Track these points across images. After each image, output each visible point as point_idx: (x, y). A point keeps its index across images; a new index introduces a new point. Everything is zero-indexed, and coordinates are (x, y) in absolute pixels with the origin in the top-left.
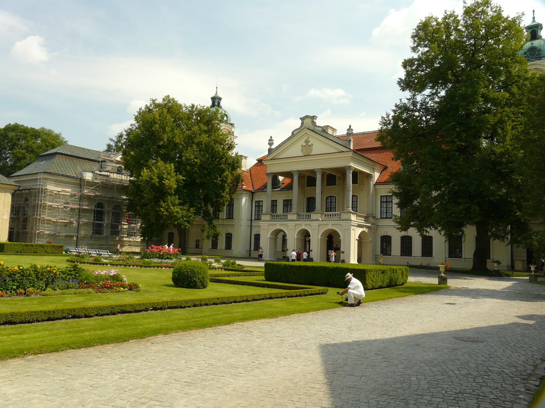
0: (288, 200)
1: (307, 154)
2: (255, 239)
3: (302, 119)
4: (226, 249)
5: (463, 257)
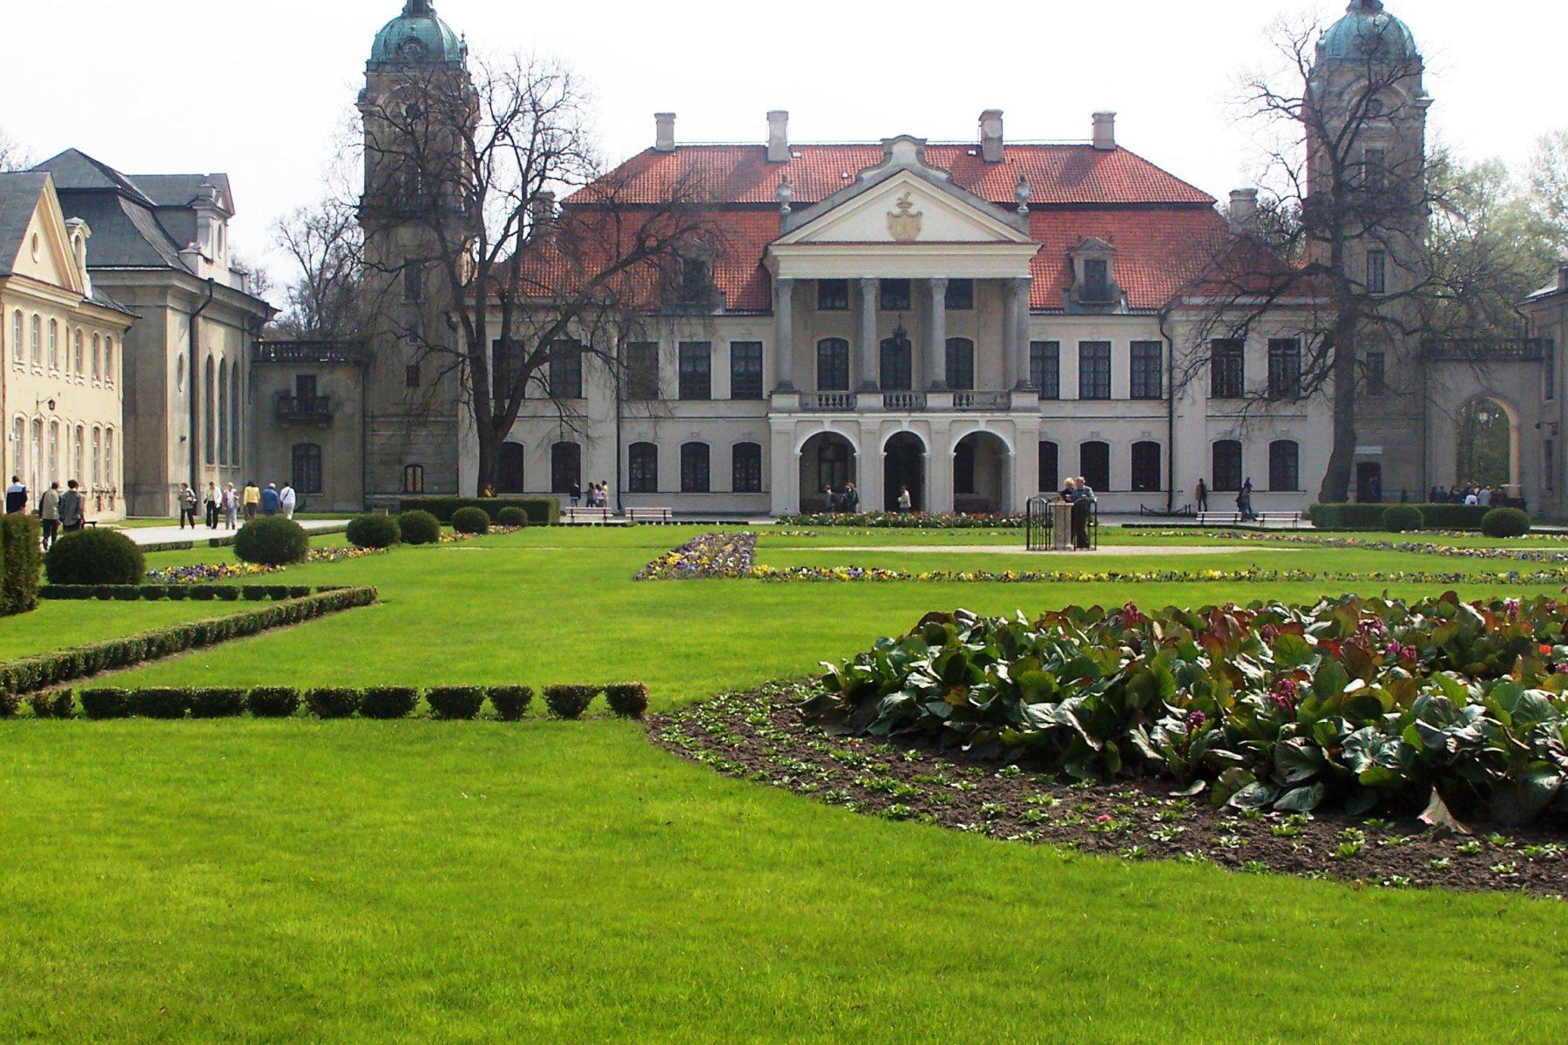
1: (902, 238)
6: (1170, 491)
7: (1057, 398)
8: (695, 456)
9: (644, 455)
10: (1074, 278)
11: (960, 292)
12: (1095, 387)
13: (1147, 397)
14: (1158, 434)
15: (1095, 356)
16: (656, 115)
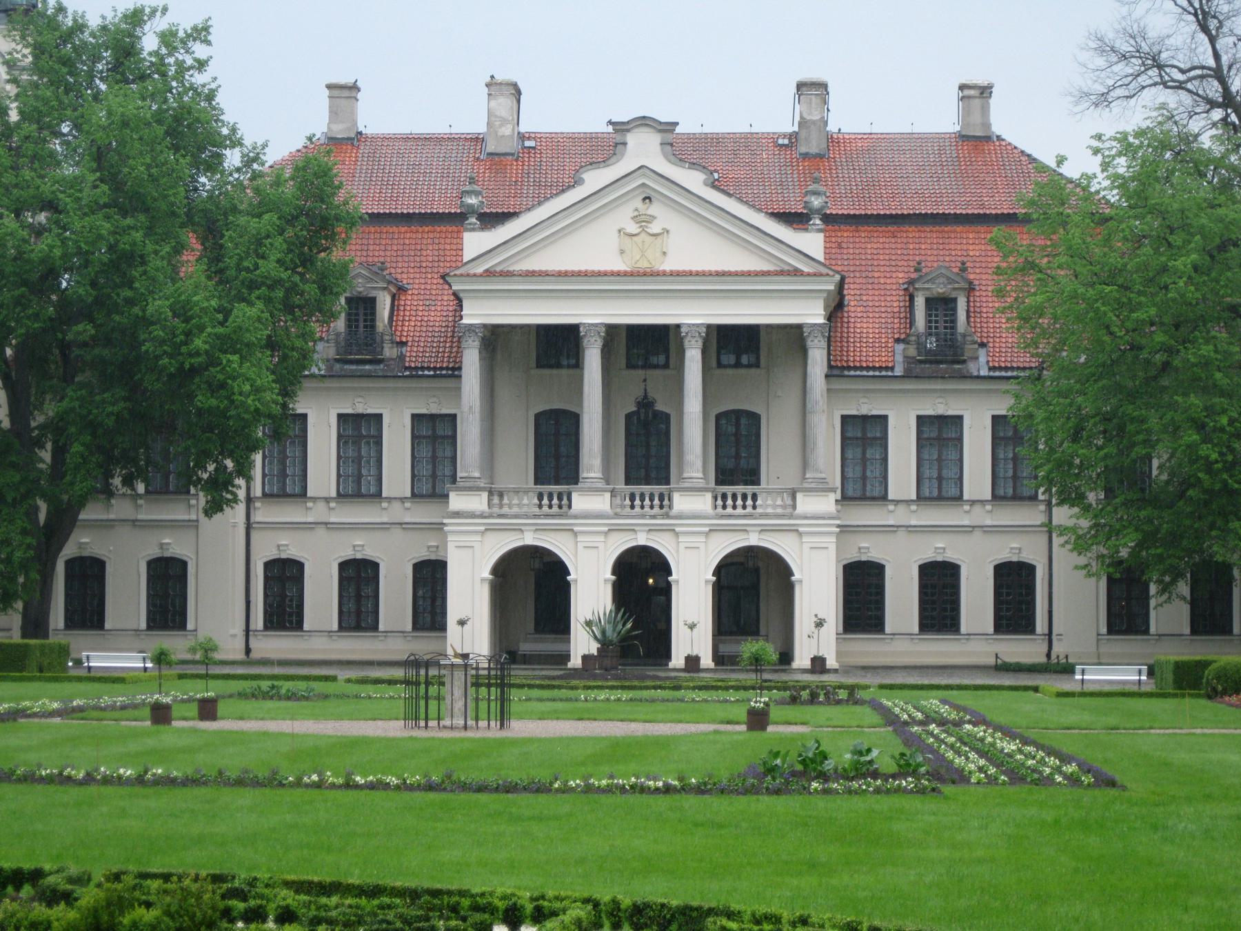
0: (432, 417)
1: (643, 265)
2: (266, 578)
3: (621, 128)
4: (149, 628)
5: (1153, 630)
6: (1050, 634)
7: (884, 497)
8: (359, 578)
9: (285, 579)
10: (912, 323)
11: (735, 346)
12: (940, 484)
13: (1017, 498)
14: (1030, 551)
15: (940, 435)
16: (329, 87)
